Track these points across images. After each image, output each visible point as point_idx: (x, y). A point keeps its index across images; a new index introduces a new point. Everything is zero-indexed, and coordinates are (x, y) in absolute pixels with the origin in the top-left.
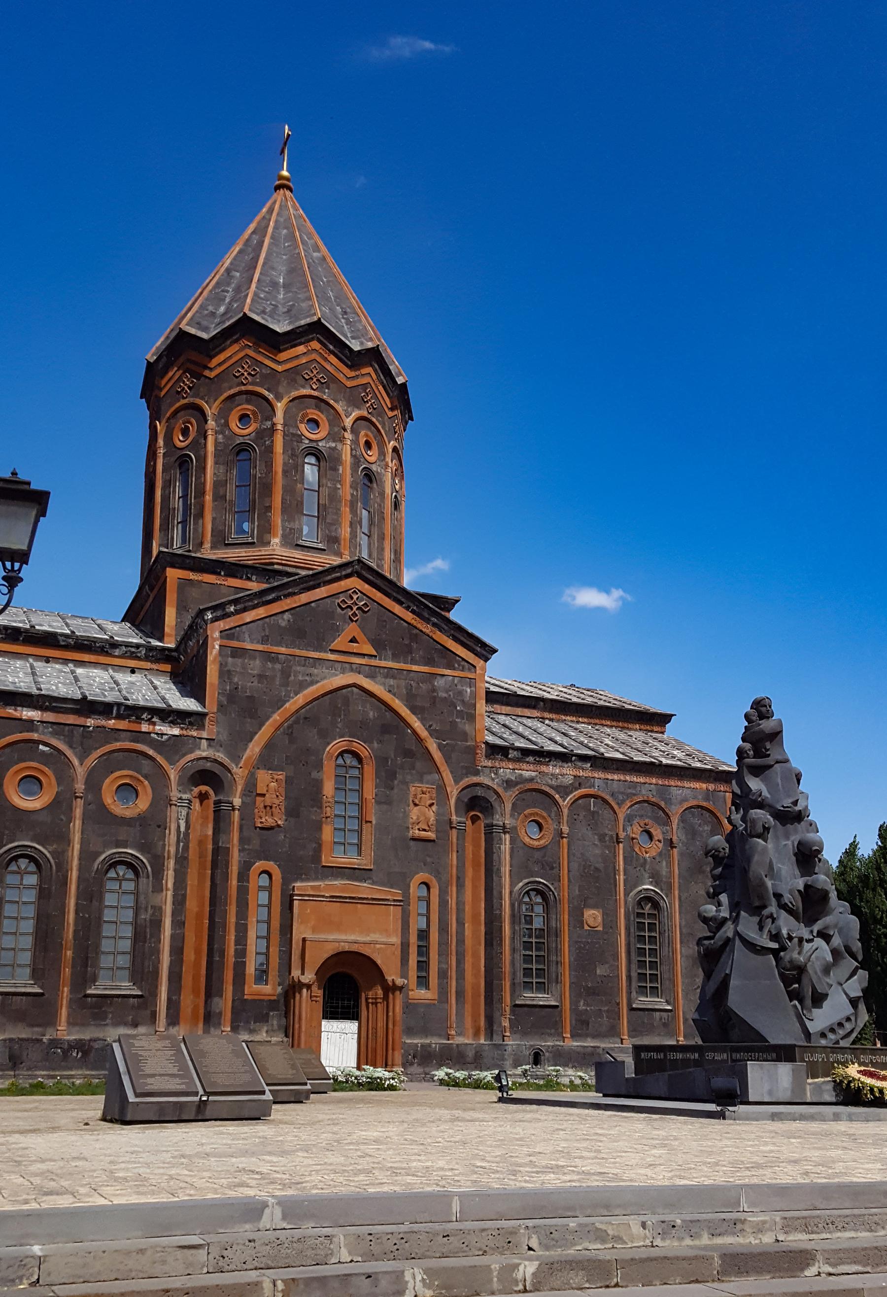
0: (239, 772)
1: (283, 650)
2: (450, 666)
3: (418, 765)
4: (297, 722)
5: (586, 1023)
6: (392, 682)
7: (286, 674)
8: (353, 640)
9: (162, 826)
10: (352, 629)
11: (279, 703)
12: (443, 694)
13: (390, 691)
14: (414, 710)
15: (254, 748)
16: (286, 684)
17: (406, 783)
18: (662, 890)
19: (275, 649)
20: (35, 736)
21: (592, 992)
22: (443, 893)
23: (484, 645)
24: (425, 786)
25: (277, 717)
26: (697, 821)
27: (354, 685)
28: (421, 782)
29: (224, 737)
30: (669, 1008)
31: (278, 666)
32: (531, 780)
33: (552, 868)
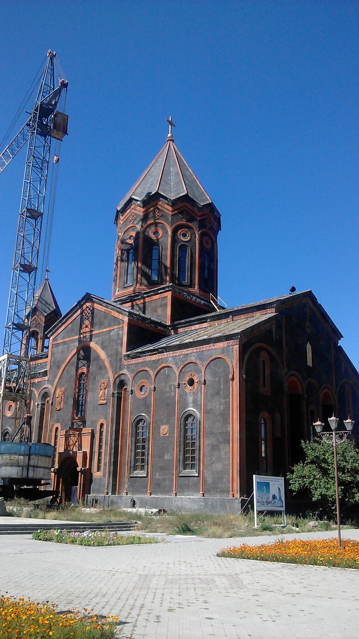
1: (68, 339)
3: (103, 371)
5: (159, 485)
6: (97, 339)
7: (68, 348)
12: (112, 338)
13: (96, 343)
14: (103, 348)
16: (68, 352)
17: (98, 381)
18: (197, 409)
21: (162, 469)
22: (107, 426)
24: (103, 381)
25: (63, 366)
28: (103, 379)
30: (197, 475)
31: (66, 346)
33: (148, 407)
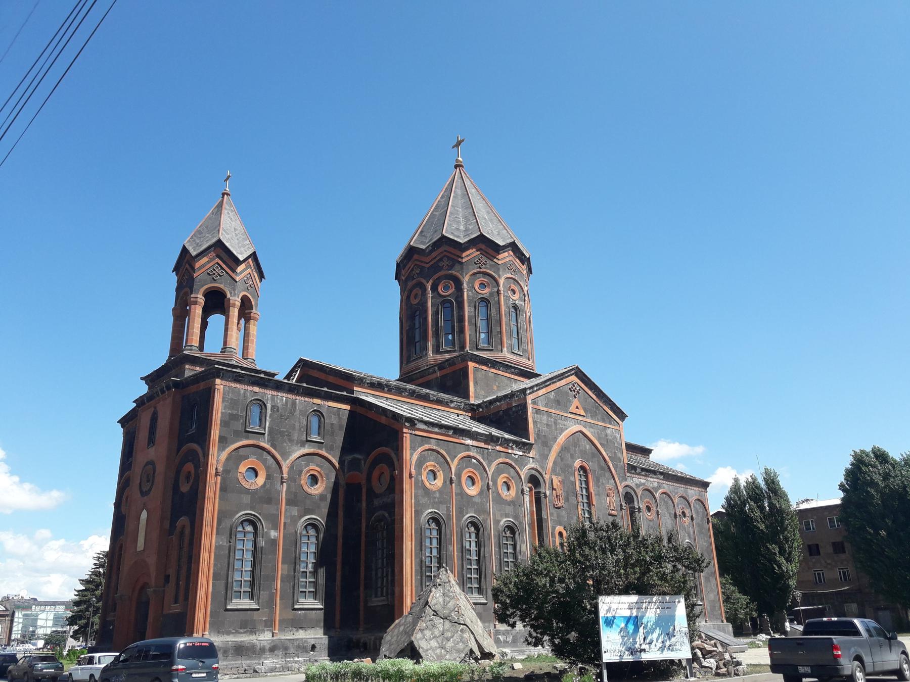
0: (547, 477)
1: (553, 411)
2: (610, 423)
4: (562, 449)
7: (556, 423)
8: (577, 408)
9: (521, 505)
10: (576, 402)
11: (555, 439)
15: (550, 464)
19: (551, 410)
20: (471, 454)
23: (623, 413)
26: (698, 507)
27: (581, 432)
29: (538, 457)
32: (644, 484)
